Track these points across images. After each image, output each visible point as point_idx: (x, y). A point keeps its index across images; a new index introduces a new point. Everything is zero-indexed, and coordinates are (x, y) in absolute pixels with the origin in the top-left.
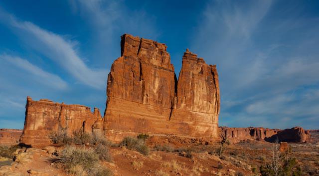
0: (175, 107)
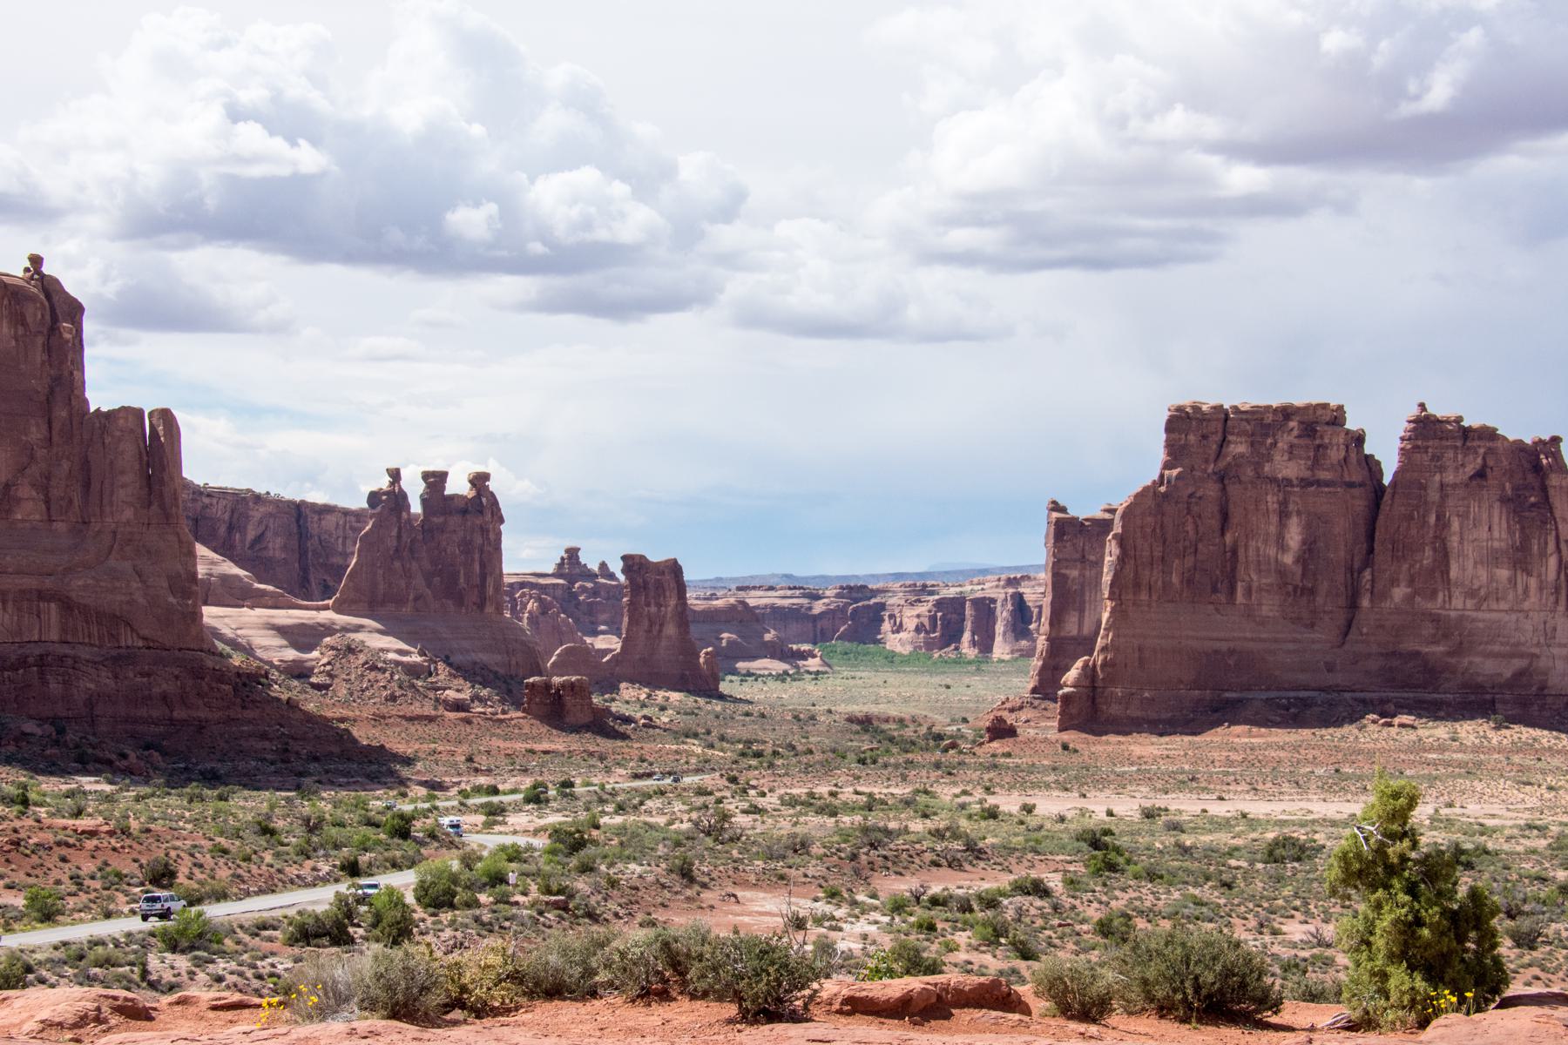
0: (1365, 602)
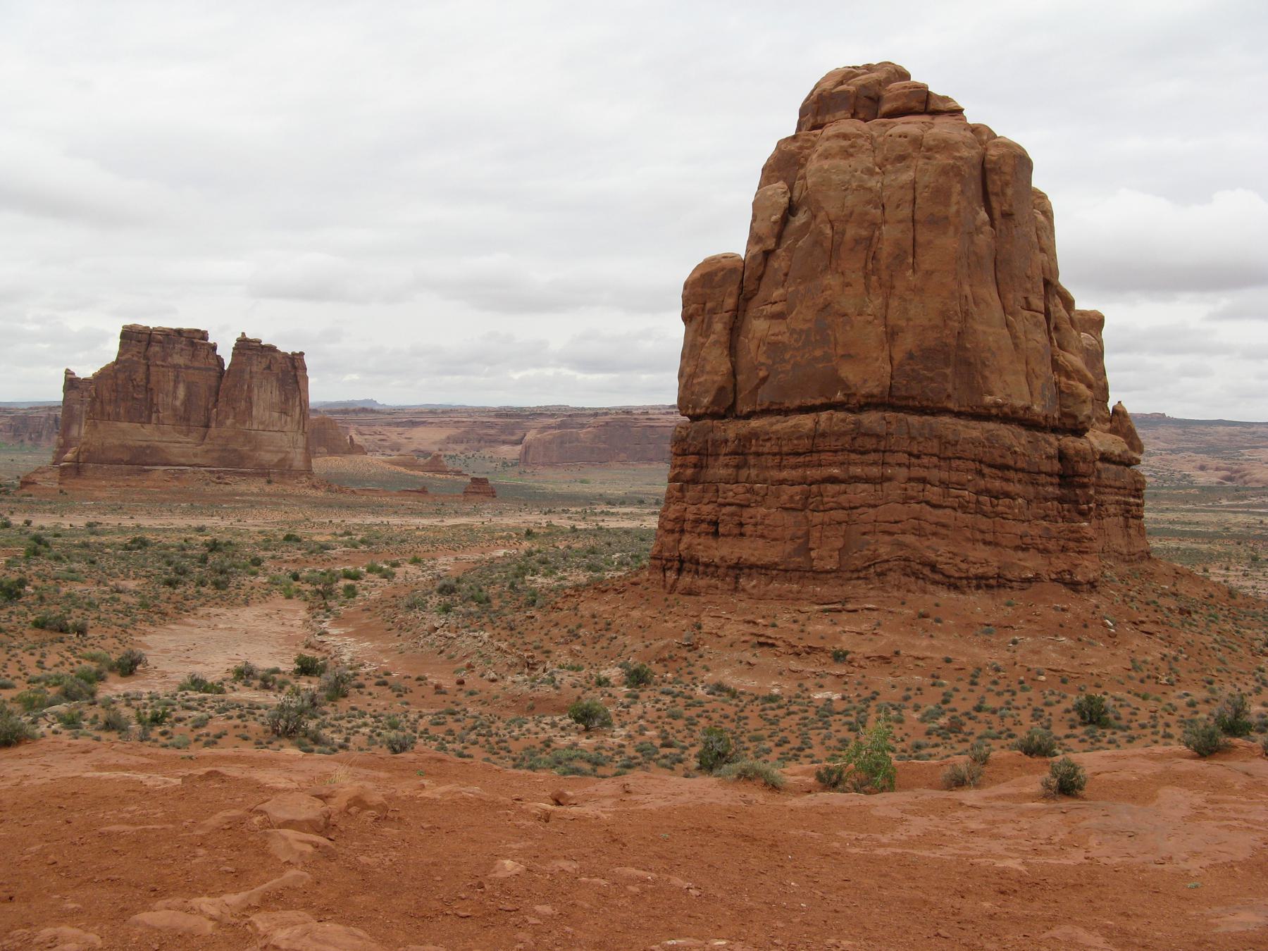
0: (213, 425)
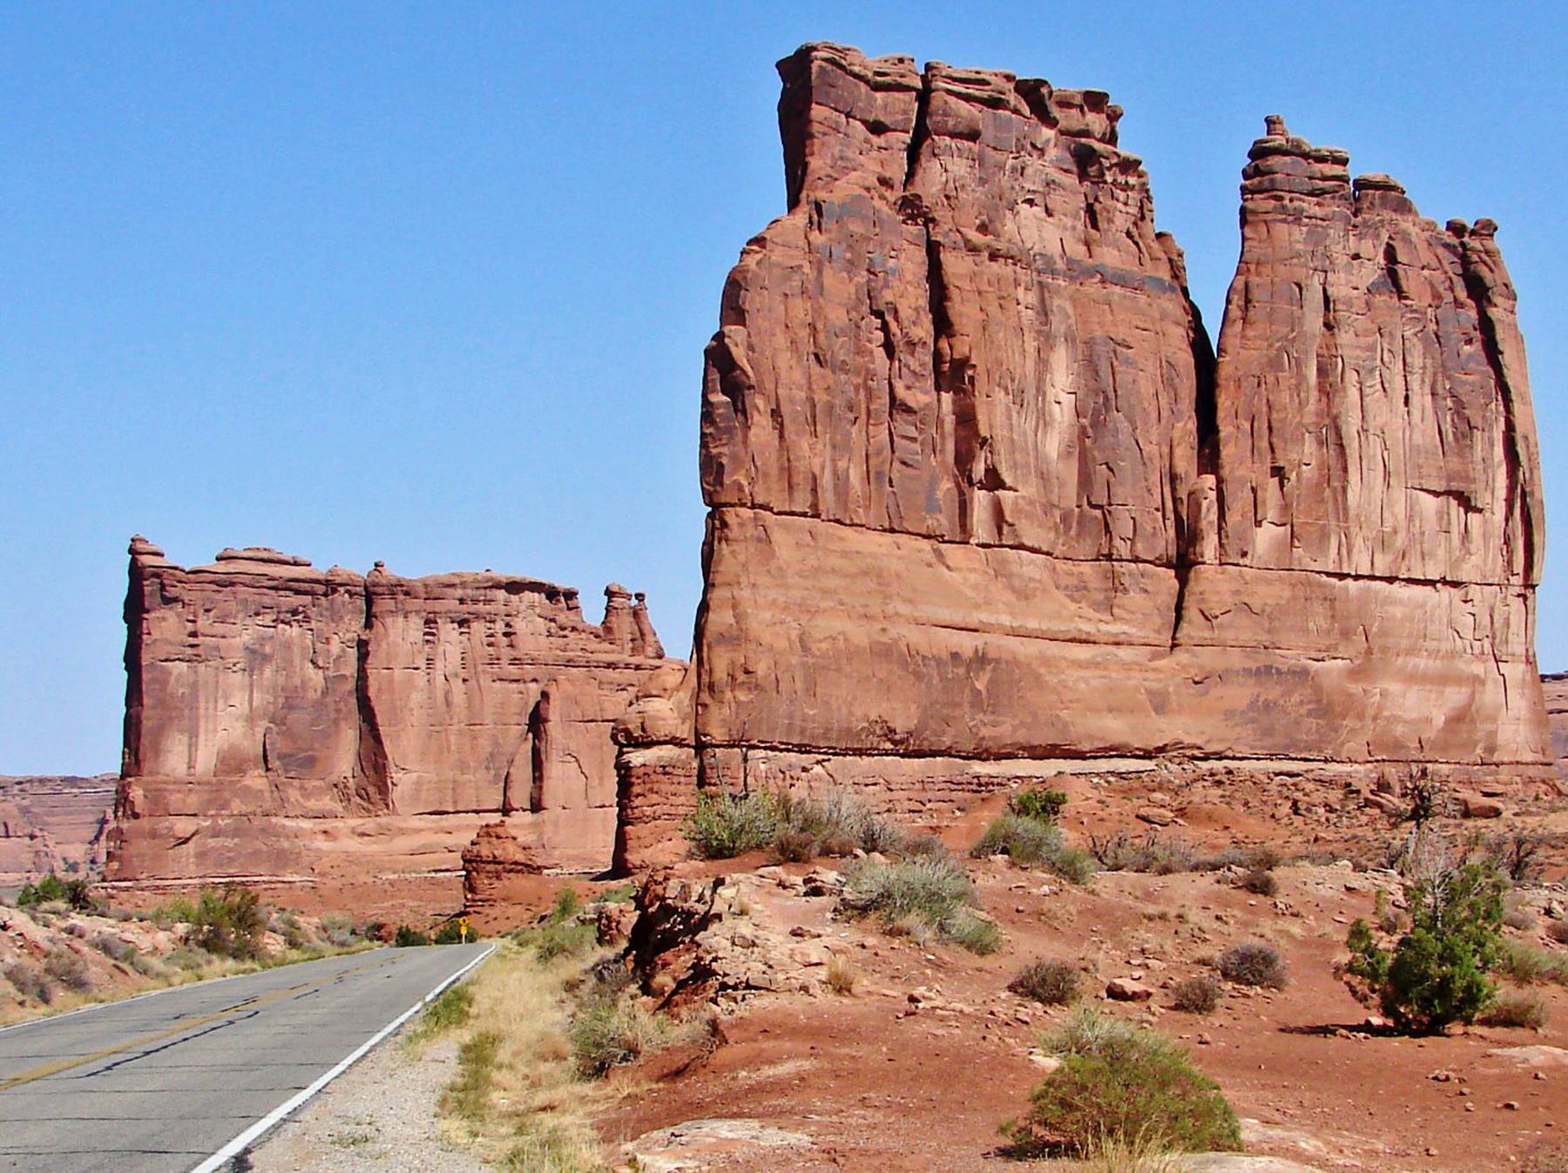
0: (1209, 548)
